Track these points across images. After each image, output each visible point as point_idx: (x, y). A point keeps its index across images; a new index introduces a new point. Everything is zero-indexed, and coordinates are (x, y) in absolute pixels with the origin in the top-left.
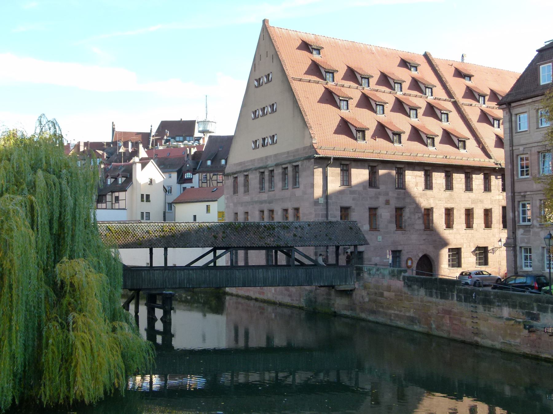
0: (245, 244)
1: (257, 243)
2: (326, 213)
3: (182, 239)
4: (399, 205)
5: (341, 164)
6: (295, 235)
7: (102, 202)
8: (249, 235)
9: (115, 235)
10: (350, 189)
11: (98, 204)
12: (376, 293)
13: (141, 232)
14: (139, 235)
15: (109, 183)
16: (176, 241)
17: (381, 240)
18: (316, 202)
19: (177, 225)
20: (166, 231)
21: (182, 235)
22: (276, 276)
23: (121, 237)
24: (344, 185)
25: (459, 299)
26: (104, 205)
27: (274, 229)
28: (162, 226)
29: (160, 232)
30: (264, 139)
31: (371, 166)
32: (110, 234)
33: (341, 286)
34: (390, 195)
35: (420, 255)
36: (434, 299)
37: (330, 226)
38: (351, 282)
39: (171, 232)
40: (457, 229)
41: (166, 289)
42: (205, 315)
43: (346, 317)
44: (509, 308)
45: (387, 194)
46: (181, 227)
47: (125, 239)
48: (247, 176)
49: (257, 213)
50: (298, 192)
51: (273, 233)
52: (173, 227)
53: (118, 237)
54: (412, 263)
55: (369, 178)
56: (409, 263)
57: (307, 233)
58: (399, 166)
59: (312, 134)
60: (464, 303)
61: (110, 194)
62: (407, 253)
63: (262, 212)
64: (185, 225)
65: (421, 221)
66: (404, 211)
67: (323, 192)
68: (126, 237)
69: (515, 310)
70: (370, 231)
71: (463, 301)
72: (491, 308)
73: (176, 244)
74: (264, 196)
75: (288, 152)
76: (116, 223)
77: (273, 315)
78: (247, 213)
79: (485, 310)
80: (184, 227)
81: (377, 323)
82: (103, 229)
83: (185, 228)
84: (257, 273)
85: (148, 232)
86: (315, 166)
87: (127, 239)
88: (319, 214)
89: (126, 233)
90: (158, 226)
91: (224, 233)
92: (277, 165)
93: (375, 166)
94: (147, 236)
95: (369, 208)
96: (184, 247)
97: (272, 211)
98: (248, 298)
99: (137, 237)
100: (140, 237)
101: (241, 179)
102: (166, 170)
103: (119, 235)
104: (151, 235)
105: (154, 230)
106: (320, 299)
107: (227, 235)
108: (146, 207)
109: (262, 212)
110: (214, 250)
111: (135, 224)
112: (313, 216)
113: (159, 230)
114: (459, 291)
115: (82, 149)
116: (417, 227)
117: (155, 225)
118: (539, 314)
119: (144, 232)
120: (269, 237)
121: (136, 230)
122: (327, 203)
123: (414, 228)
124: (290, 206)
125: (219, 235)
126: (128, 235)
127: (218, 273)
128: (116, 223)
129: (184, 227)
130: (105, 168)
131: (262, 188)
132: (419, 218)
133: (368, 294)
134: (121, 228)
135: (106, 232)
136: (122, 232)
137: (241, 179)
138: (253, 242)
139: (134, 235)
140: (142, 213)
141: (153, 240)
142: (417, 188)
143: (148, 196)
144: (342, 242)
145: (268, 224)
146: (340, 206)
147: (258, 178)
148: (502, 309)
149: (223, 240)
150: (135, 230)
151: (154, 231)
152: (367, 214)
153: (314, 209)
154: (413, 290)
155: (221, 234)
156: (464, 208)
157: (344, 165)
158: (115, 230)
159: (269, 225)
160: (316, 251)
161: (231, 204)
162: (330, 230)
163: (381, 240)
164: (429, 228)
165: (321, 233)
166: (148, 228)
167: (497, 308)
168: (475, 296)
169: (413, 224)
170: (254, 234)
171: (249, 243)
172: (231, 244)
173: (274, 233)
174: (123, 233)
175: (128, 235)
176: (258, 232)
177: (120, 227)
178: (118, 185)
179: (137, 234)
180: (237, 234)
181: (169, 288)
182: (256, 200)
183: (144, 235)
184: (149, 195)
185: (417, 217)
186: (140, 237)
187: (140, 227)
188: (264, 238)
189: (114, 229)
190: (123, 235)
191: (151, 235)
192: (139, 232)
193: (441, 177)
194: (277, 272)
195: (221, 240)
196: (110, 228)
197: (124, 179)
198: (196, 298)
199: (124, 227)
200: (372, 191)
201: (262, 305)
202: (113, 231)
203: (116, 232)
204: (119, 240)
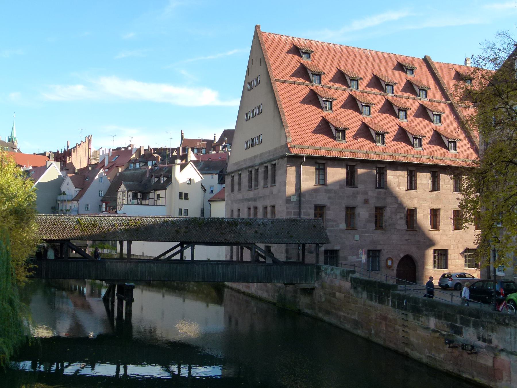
0: (204, 240)
1: (217, 239)
2: (298, 211)
4: (379, 205)
6: (256, 232)
7: (146, 200)
8: (211, 231)
9: (83, 227)
10: (325, 187)
11: (143, 201)
12: (330, 294)
13: (108, 225)
14: (105, 228)
16: (138, 234)
17: (358, 239)
18: (288, 200)
20: (132, 225)
21: (146, 229)
22: (236, 272)
23: (88, 229)
24: (320, 183)
25: (393, 306)
26: (147, 202)
27: (236, 225)
28: (129, 220)
29: (126, 225)
30: (253, 140)
31: (378, 167)
32: (78, 226)
33: (300, 285)
34: (369, 194)
35: (402, 255)
36: (373, 303)
37: (293, 224)
38: (312, 281)
39: (136, 225)
40: (444, 231)
42: (207, 306)
43: (307, 315)
44: (435, 318)
45: (366, 193)
46: (147, 221)
47: (91, 231)
48: (240, 174)
49: (246, 210)
50: (275, 190)
51: (234, 230)
52: (139, 221)
53: (85, 229)
54: (392, 263)
55: (347, 177)
56: (389, 263)
57: (269, 230)
58: (379, 166)
59: (287, 133)
60: (397, 309)
61: (153, 191)
62: (387, 252)
63: (249, 209)
64: (151, 220)
65: (403, 222)
66: (385, 210)
68: (93, 229)
69: (440, 321)
70: (346, 229)
71: (396, 307)
72: (419, 317)
73: (138, 237)
74: (251, 194)
75: (269, 151)
76: (86, 216)
77: (255, 309)
78: (239, 210)
79: (414, 319)
80: (149, 221)
81: (330, 324)
82: (74, 221)
83: (150, 223)
84: (217, 268)
85: (114, 225)
87: (94, 231)
89: (93, 226)
90: (125, 220)
91: (186, 228)
92: (261, 164)
93: (384, 168)
94: (112, 229)
95: (346, 207)
97: (256, 208)
98: (238, 291)
99: (103, 230)
100: (106, 230)
101: (236, 178)
102: (203, 172)
103: (87, 228)
104: (116, 228)
105: (120, 223)
106: (289, 296)
107: (189, 230)
108: (183, 204)
109: (249, 209)
110: (181, 245)
111: (104, 218)
112: (285, 213)
113: (125, 223)
114: (394, 296)
115: (142, 153)
116: (398, 227)
117: (123, 219)
118: (461, 328)
119: (111, 225)
120: (230, 233)
122: (300, 201)
123: (395, 228)
124: (268, 203)
125: (182, 230)
126: (95, 227)
128: (86, 216)
129: (149, 221)
130: (151, 169)
131: (250, 187)
132: (401, 218)
133: (325, 294)
134: (90, 221)
135: (75, 224)
136: (90, 224)
137: (236, 178)
138: (213, 237)
139: (101, 228)
140: (180, 210)
141: (118, 233)
142: (399, 188)
143: (186, 195)
144: (303, 240)
146: (314, 205)
147: (248, 177)
148: (429, 320)
149: (184, 235)
150: (102, 223)
151: (120, 225)
152: (344, 213)
153: (286, 207)
154: (357, 292)
155: (184, 229)
156: (452, 209)
157: (321, 165)
158: (84, 223)
159: (233, 222)
161: (230, 202)
163: (358, 239)
164: (413, 229)
166: (115, 221)
167: (425, 318)
168: (406, 303)
169: (395, 225)
170: (216, 230)
171: (209, 238)
172: (191, 239)
173: (236, 229)
174: (91, 226)
175: (95, 227)
176: (220, 227)
177: (89, 220)
178: (161, 184)
179: (104, 226)
180: (199, 229)
182: (246, 198)
183: (110, 228)
184: (188, 193)
185: (398, 217)
186: (106, 230)
187: (108, 220)
188: (225, 234)
189: (84, 221)
190: (91, 228)
191: (116, 228)
192: (106, 225)
193: (426, 177)
195: (182, 235)
196: (80, 221)
197: (165, 179)
198: (201, 289)
199: (93, 220)
200: (350, 190)
201: (249, 299)
202: (82, 224)
203: (84, 225)
204: (86, 232)
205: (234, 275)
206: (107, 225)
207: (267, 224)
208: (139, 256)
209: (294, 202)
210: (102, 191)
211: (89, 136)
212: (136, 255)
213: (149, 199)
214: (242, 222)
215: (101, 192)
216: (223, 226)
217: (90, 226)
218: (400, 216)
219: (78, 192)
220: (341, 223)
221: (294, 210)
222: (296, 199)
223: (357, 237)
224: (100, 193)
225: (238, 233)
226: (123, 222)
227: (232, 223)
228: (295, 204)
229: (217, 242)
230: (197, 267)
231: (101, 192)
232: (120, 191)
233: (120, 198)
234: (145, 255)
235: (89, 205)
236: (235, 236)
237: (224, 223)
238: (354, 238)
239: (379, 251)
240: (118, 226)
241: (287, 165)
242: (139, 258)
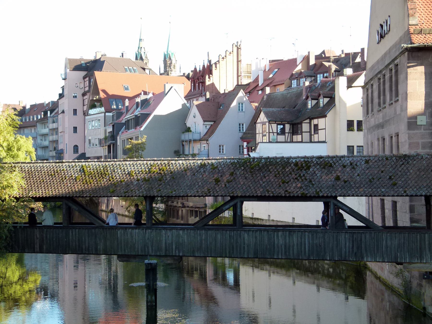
1: (273, 190)
3: (170, 184)
6: (338, 178)
8: (267, 178)
11: (294, 136)
14: (116, 178)
15: (309, 107)
16: (160, 186)
19: (172, 163)
20: (154, 172)
23: (93, 181)
26: (299, 138)
27: (309, 168)
28: (151, 166)
32: (81, 176)
37: (401, 163)
41: (148, 256)
46: (176, 165)
51: (304, 175)
52: (165, 166)
57: (358, 175)
59: (411, 9)
61: (308, 121)
64: (183, 163)
67: (425, 106)
82: (77, 169)
85: (129, 174)
86: (408, 63)
87: (101, 183)
88: (418, 143)
89: (102, 176)
90: (146, 166)
99: (113, 181)
100: (117, 180)
103: (92, 178)
105: (139, 171)
107: (234, 178)
115: (312, 62)
117: (143, 164)
119: (125, 173)
121: (116, 171)
127: (219, 236)
135: (78, 174)
144: (413, 190)
145: (303, 160)
149: (226, 185)
150: (114, 171)
151: (137, 173)
155: (227, 176)
160: (413, 204)
162: (400, 169)
165: (382, 174)
166: (132, 168)
173: (306, 175)
174: (98, 176)
176: (282, 172)
178: (319, 109)
179: (115, 176)
181: (150, 255)
186: (117, 180)
187: (123, 166)
188: (287, 183)
190: (97, 178)
191: (132, 178)
192: (118, 173)
194: (307, 237)
195: (223, 186)
196: (85, 169)
197: (326, 100)
202: (87, 173)
203: (90, 174)
204: (90, 185)
205: (303, 248)
206: (120, 173)
207: (358, 164)
208: (264, 221)
209: (423, 127)
210: (243, 125)
211: (237, 42)
212: (261, 219)
214: (319, 162)
215: (241, 126)
216: (287, 170)
217: (97, 175)
219: (208, 127)
221: (423, 141)
222: (427, 122)
224: (240, 128)
225: (308, 180)
226: (143, 168)
227: (302, 165)
228: (424, 130)
230: (246, 235)
231: (241, 126)
233: (259, 133)
234: (271, 219)
235: (225, 147)
236: (303, 185)
237: (290, 165)
240: (135, 175)
241: (408, 65)
242: (264, 223)
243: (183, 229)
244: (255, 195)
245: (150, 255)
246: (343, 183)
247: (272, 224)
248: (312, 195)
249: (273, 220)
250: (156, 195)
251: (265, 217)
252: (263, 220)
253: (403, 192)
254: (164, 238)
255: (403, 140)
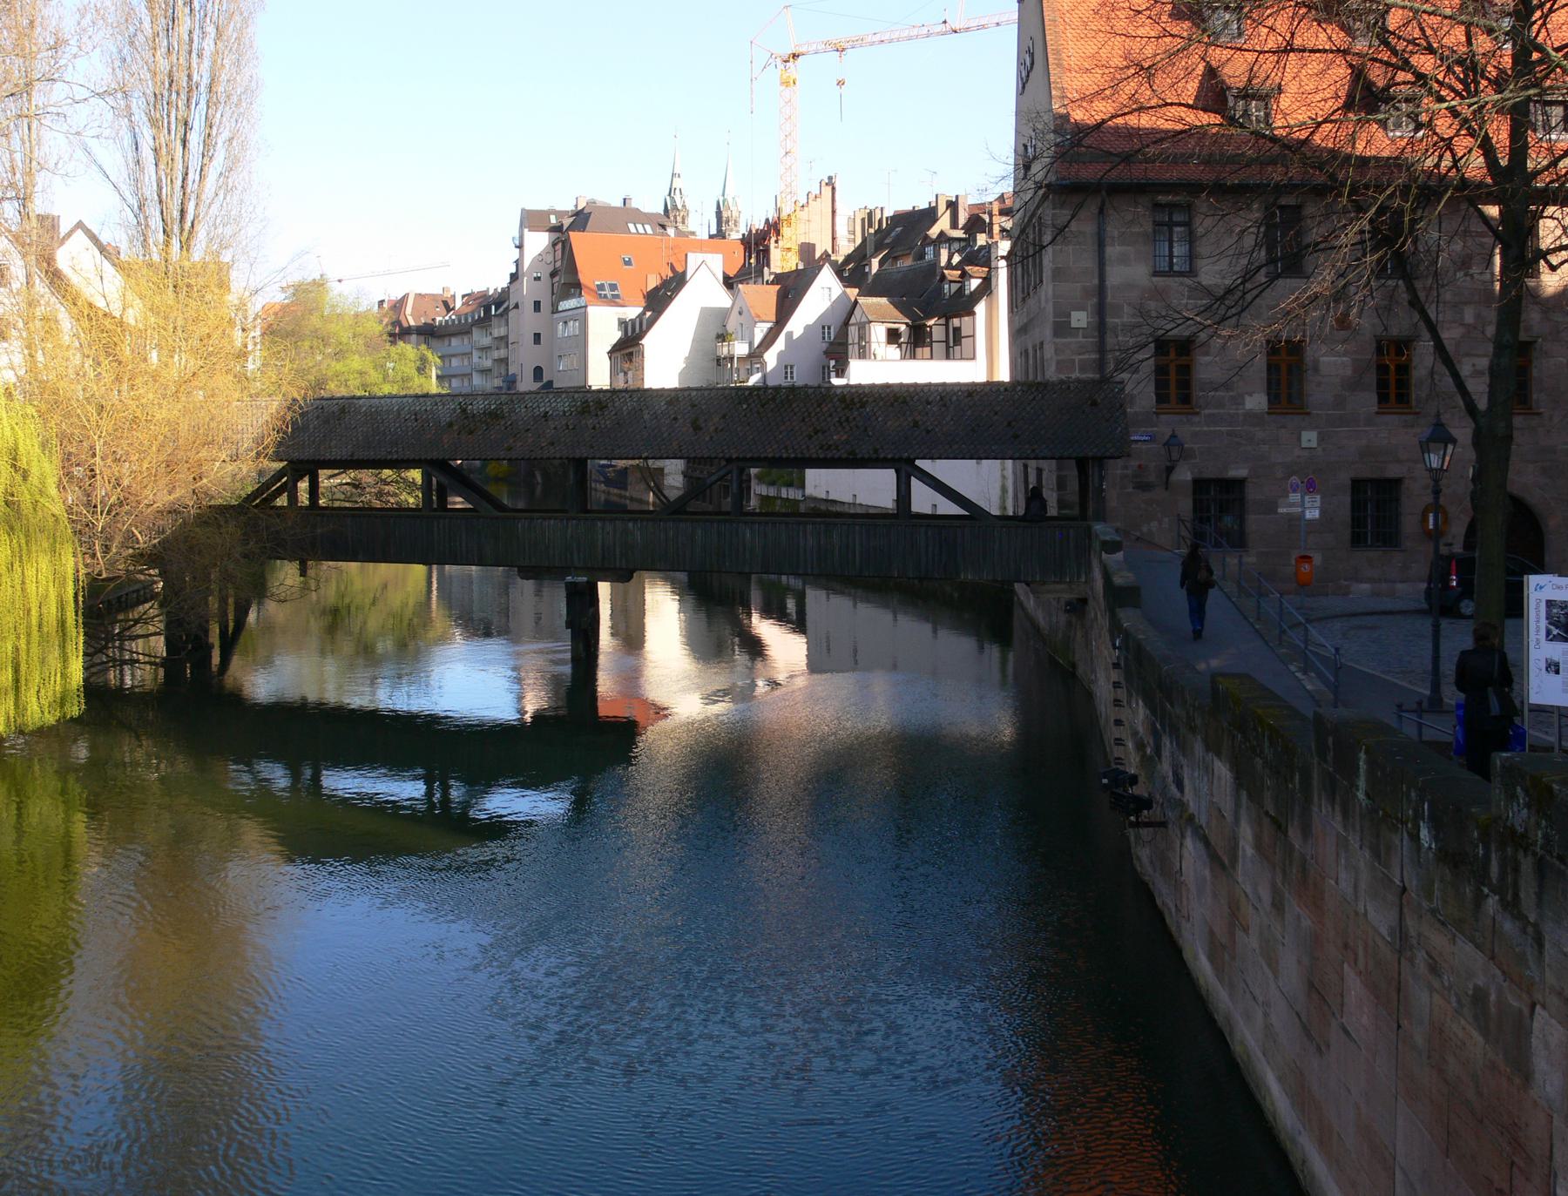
5: (1157, 206)
6: (916, 424)
8: (788, 423)
17: (1314, 444)
37: (1031, 397)
96: (951, 456)
127: (699, 532)
163: (1314, 444)
164: (1530, 409)
165: (996, 417)
195: (707, 439)
208: (846, 506)
210: (829, 328)
213: (932, 342)
216: (825, 409)
218: (1474, 365)
219: (765, 330)
220: (1251, 395)
223: (1310, 438)
224: (824, 333)
228: (1084, 337)
229: (796, 458)
230: (748, 531)
232: (853, 325)
233: (853, 344)
234: (858, 502)
235: (795, 369)
238: (1299, 439)
239: (1398, 482)
242: (846, 509)
243: (635, 520)
244: (762, 456)
245: (576, 568)
246: (924, 433)
247: (859, 511)
248: (866, 456)
249: (861, 505)
250: (585, 455)
251: (848, 499)
252: (844, 503)
253: (1029, 452)
254: (600, 537)
255: (1049, 356)
